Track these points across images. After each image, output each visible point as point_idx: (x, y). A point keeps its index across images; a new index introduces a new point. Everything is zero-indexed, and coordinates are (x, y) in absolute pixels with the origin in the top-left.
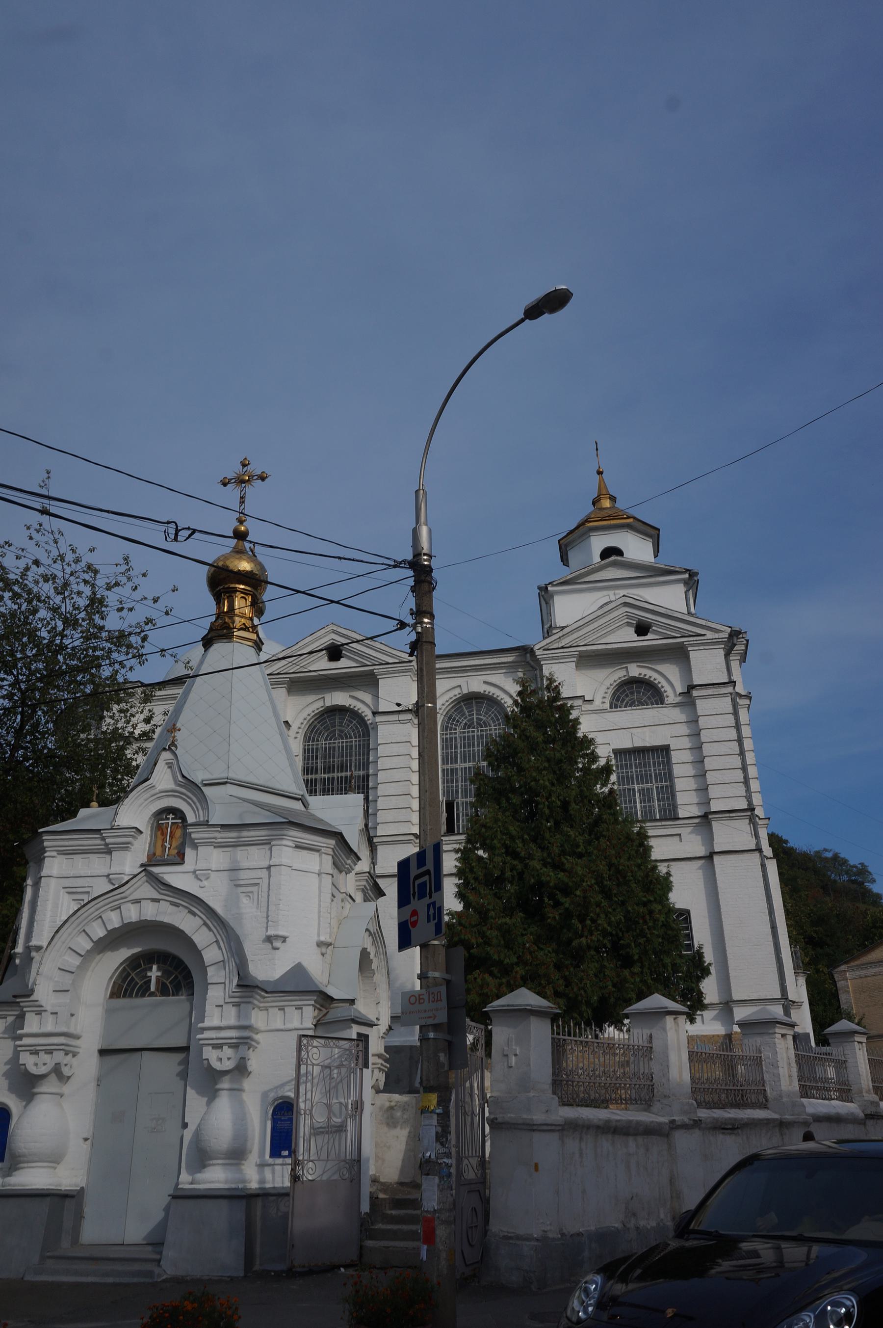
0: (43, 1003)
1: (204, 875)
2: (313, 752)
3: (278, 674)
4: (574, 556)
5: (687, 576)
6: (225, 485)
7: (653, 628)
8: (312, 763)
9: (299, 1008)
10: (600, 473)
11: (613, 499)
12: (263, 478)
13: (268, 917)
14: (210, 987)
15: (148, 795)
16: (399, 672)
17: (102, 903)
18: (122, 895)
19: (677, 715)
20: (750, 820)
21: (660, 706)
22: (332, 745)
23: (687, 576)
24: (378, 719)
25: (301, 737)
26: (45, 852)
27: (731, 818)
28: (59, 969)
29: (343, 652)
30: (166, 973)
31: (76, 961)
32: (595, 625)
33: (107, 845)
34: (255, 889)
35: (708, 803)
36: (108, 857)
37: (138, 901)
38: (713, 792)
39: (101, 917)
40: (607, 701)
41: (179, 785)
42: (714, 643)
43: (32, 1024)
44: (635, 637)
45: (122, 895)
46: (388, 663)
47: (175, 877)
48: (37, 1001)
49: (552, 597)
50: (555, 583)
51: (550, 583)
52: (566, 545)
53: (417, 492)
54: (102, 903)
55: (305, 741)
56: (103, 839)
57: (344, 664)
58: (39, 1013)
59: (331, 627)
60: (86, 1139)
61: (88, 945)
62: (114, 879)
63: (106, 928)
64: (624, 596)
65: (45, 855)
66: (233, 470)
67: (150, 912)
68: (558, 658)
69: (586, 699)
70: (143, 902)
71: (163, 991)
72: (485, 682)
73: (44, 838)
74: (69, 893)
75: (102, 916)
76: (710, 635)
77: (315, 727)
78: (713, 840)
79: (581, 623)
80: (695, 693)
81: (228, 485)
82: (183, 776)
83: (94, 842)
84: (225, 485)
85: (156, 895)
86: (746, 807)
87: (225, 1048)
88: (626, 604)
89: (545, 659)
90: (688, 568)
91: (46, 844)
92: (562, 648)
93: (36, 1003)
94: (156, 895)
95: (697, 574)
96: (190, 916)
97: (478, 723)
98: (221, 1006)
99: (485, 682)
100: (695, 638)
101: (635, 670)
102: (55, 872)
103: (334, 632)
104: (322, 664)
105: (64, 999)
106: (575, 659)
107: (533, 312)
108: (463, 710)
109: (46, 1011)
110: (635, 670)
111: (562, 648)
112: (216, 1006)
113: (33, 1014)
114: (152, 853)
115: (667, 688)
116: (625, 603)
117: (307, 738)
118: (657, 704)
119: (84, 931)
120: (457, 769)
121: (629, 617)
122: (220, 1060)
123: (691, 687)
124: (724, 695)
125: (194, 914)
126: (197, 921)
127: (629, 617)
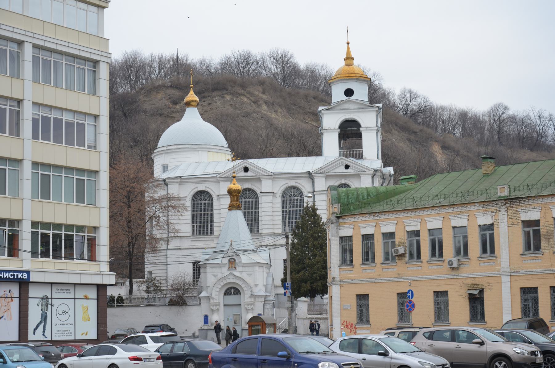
10: (348, 43)
16: (268, 178)
24: (262, 194)
30: (235, 291)
32: (332, 165)
37: (229, 278)
42: (369, 174)
43: (212, 301)
46: (265, 176)
47: (236, 273)
51: (322, 110)
67: (232, 280)
71: (234, 294)
79: (327, 165)
83: (218, 265)
89: (315, 177)
92: (320, 173)
100: (361, 173)
105: (217, 297)
111: (320, 173)
121: (342, 162)
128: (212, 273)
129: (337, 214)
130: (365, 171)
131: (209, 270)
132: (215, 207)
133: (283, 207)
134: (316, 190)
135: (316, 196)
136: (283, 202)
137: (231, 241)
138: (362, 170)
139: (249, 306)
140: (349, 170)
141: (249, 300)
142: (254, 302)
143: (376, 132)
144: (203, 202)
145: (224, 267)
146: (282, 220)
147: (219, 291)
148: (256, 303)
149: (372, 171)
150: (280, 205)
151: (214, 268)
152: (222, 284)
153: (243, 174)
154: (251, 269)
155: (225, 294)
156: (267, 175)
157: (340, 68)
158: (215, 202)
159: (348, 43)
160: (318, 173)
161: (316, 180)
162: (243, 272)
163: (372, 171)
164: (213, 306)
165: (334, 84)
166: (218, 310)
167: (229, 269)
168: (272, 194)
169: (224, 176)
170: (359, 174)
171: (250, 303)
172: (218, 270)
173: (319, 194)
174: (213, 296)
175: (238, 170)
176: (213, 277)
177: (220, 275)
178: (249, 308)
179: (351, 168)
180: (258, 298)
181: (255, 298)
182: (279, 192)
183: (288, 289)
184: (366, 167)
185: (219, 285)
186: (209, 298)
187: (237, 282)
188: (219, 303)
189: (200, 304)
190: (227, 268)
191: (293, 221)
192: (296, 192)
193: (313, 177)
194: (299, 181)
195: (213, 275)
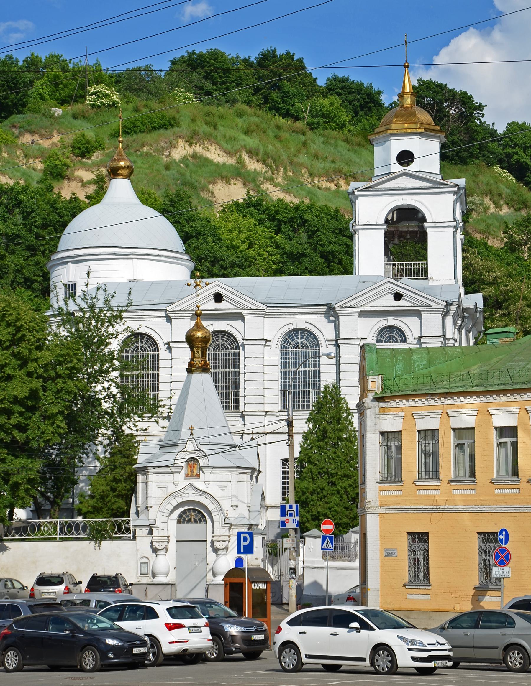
21: (404, 343)
23: (456, 189)
24: (245, 342)
40: (375, 338)
42: (436, 310)
47: (198, 484)
49: (357, 197)
50: (360, 189)
51: (356, 189)
57: (224, 305)
68: (348, 313)
76: (435, 306)
85: (193, 492)
89: (341, 313)
97: (301, 346)
101: (391, 321)
103: (218, 285)
108: (293, 337)
110: (391, 321)
118: (403, 342)
120: (289, 371)
123: (421, 337)
126: (209, 501)
128: (158, 484)
129: (376, 393)
130: (431, 306)
132: (161, 363)
133: (283, 366)
134: (341, 337)
136: (284, 356)
137: (192, 428)
139: (221, 543)
140: (402, 302)
141: (222, 532)
143: (452, 230)
144: (140, 353)
146: (280, 389)
149: (441, 305)
150: (278, 362)
152: (175, 503)
155: (179, 522)
156: (256, 308)
158: (163, 353)
160: (346, 307)
161: (342, 319)
163: (441, 305)
165: (379, 141)
168: (263, 342)
169: (178, 309)
170: (418, 310)
177: (171, 488)
179: (404, 299)
181: (230, 529)
182: (276, 339)
183: (291, 515)
187: (202, 499)
188: (168, 537)
189: (134, 538)
191: (300, 390)
192: (306, 340)
193: (337, 314)
194: (311, 319)
195: (159, 487)
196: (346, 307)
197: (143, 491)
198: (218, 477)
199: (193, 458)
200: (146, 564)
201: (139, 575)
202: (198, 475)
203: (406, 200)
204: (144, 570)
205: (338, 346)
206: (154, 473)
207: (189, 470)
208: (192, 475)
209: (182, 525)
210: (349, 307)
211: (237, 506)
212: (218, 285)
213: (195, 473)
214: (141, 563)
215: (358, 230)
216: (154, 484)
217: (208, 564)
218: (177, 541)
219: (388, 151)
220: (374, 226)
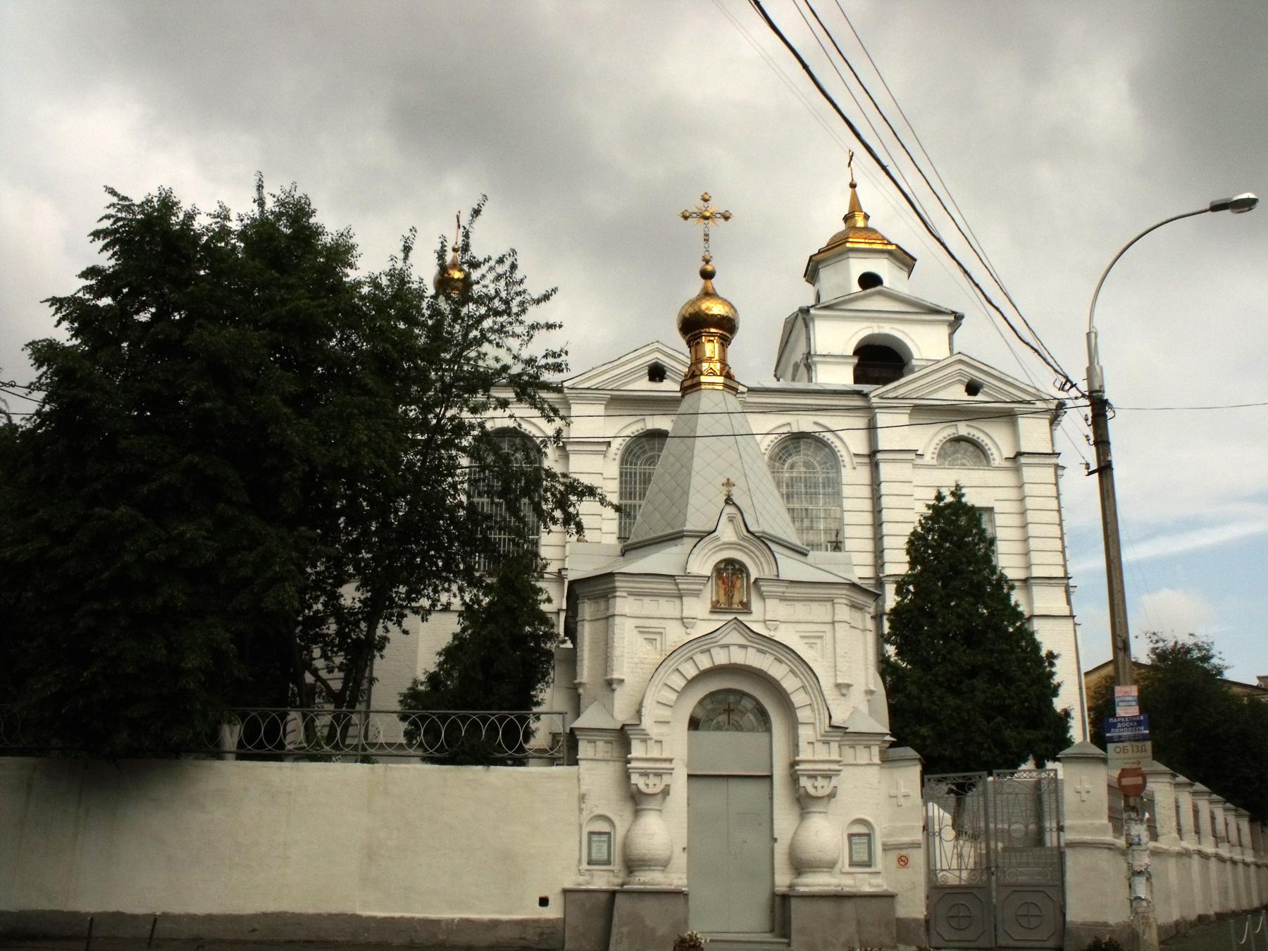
0: (648, 732)
1: (774, 625)
2: (631, 477)
3: (596, 389)
4: (825, 274)
5: (952, 318)
6: (686, 218)
7: (985, 389)
8: (630, 488)
9: (868, 747)
10: (853, 186)
11: (867, 217)
12: (726, 218)
13: (836, 666)
14: (800, 726)
15: (712, 546)
17: (695, 646)
18: (713, 640)
19: (1007, 478)
20: (1066, 587)
22: (629, 470)
23: (952, 318)
25: (618, 458)
26: (615, 591)
27: (1051, 585)
28: (658, 702)
29: (667, 373)
31: (674, 696)
33: (679, 590)
34: (818, 641)
35: (1028, 567)
36: (677, 602)
37: (727, 646)
38: (1035, 558)
39: (692, 658)
41: (743, 539)
43: (637, 750)
44: (965, 397)
45: (713, 640)
48: (644, 730)
49: (813, 320)
52: (818, 263)
53: (1088, 334)
54: (695, 646)
55: (622, 464)
56: (677, 584)
58: (644, 741)
59: (657, 345)
60: (684, 849)
61: (683, 683)
62: (690, 622)
63: (698, 668)
64: (960, 353)
65: (618, 594)
66: (695, 205)
67: (739, 657)
69: (918, 453)
70: (731, 648)
72: (816, 423)
73: (617, 578)
74: (640, 632)
75: (694, 657)
76: (1039, 405)
77: (632, 450)
78: (1033, 604)
80: (1023, 460)
81: (689, 219)
82: (748, 531)
83: (668, 586)
84: (686, 218)
85: (744, 642)
86: (1062, 575)
87: (819, 778)
88: (961, 361)
90: (954, 310)
91: (617, 584)
92: (893, 398)
93: (644, 732)
94: (743, 641)
95: (962, 317)
96: (776, 663)
98: (813, 743)
99: (816, 423)
101: (963, 429)
102: (627, 611)
104: (643, 385)
106: (909, 412)
107: (1216, 208)
109: (651, 739)
110: (963, 429)
111: (896, 398)
112: (809, 743)
113: (638, 741)
114: (714, 599)
115: (993, 451)
116: (960, 360)
117: (624, 461)
119: (677, 669)
121: (961, 374)
122: (816, 788)
123: (1019, 454)
124: (1048, 465)
125: (780, 661)
127: (961, 374)
131: (624, 605)
135: (882, 466)
138: (1017, 399)
139: (820, 782)
140: (980, 397)
141: (821, 753)
142: (838, 762)
145: (696, 594)
147: (678, 698)
148: (846, 773)
151: (647, 600)
152: (691, 672)
153: (643, 385)
154: (820, 612)
155: (694, 724)
157: (835, 236)
159: (853, 186)
160: (889, 398)
161: (882, 419)
162: (782, 626)
164: (645, 774)
165: (827, 264)
166: (666, 792)
167: (716, 609)
171: (826, 766)
172: (667, 607)
173: (894, 460)
174: (647, 723)
175: (631, 372)
176: (640, 639)
177: (675, 635)
178: (820, 793)
180: (852, 747)
184: (1033, 391)
185: (677, 673)
186: (622, 737)
188: (670, 760)
190: (709, 606)
195: (641, 630)
196: (889, 398)
197: (594, 642)
198: (799, 611)
199: (730, 562)
200: (605, 838)
201: (585, 866)
202: (746, 608)
203: (883, 327)
204: (600, 852)
205: (874, 466)
206: (631, 594)
207: (722, 592)
208: (731, 603)
209: (701, 735)
210: (893, 398)
211: (848, 686)
212: (658, 350)
213: (736, 599)
214: (591, 833)
215: (815, 363)
216: (630, 624)
217: (775, 840)
218: (690, 776)
219: (847, 271)
220: (838, 358)
